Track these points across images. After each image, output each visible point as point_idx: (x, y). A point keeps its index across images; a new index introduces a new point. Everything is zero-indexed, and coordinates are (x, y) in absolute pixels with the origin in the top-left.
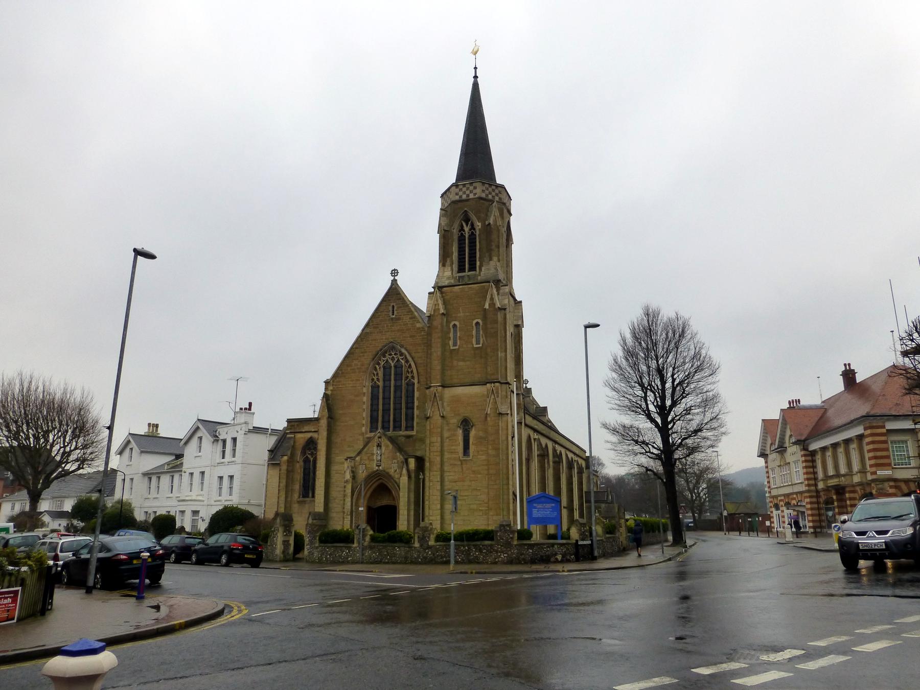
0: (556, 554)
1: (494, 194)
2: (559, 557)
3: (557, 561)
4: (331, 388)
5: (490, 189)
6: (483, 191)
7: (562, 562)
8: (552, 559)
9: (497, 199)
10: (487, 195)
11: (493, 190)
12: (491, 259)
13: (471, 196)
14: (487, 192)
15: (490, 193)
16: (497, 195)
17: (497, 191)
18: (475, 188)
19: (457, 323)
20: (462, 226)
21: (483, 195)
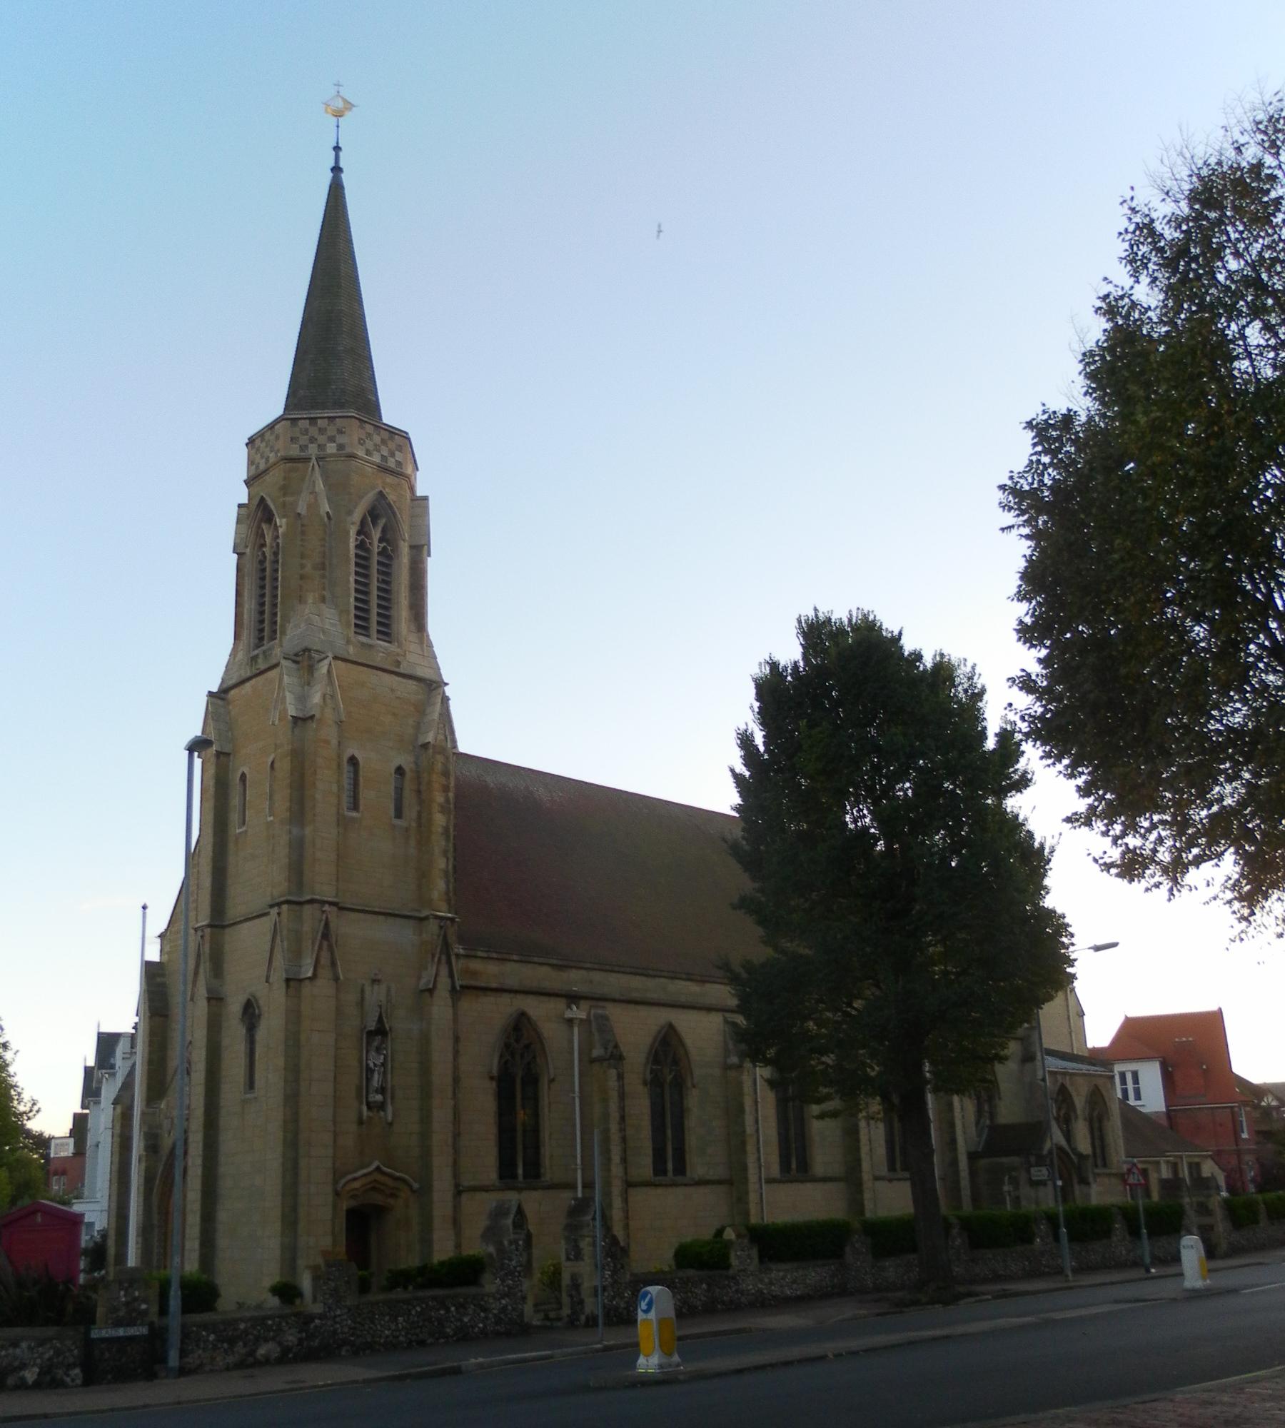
0: (23, 1366)
1: (322, 439)
2: (30, 1375)
3: (22, 1386)
4: (167, 949)
5: (313, 431)
6: (293, 440)
7: (37, 1385)
8: (11, 1381)
9: (331, 448)
10: (303, 448)
11: (322, 431)
12: (301, 600)
13: (272, 459)
14: (304, 440)
15: (313, 440)
16: (332, 439)
17: (331, 431)
18: (277, 438)
19: (246, 770)
20: (263, 536)
21: (294, 451)
